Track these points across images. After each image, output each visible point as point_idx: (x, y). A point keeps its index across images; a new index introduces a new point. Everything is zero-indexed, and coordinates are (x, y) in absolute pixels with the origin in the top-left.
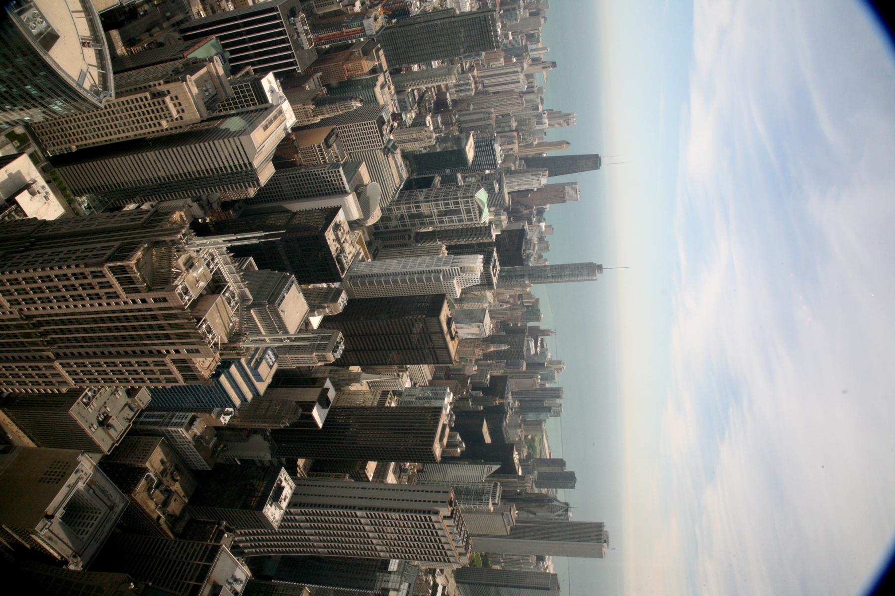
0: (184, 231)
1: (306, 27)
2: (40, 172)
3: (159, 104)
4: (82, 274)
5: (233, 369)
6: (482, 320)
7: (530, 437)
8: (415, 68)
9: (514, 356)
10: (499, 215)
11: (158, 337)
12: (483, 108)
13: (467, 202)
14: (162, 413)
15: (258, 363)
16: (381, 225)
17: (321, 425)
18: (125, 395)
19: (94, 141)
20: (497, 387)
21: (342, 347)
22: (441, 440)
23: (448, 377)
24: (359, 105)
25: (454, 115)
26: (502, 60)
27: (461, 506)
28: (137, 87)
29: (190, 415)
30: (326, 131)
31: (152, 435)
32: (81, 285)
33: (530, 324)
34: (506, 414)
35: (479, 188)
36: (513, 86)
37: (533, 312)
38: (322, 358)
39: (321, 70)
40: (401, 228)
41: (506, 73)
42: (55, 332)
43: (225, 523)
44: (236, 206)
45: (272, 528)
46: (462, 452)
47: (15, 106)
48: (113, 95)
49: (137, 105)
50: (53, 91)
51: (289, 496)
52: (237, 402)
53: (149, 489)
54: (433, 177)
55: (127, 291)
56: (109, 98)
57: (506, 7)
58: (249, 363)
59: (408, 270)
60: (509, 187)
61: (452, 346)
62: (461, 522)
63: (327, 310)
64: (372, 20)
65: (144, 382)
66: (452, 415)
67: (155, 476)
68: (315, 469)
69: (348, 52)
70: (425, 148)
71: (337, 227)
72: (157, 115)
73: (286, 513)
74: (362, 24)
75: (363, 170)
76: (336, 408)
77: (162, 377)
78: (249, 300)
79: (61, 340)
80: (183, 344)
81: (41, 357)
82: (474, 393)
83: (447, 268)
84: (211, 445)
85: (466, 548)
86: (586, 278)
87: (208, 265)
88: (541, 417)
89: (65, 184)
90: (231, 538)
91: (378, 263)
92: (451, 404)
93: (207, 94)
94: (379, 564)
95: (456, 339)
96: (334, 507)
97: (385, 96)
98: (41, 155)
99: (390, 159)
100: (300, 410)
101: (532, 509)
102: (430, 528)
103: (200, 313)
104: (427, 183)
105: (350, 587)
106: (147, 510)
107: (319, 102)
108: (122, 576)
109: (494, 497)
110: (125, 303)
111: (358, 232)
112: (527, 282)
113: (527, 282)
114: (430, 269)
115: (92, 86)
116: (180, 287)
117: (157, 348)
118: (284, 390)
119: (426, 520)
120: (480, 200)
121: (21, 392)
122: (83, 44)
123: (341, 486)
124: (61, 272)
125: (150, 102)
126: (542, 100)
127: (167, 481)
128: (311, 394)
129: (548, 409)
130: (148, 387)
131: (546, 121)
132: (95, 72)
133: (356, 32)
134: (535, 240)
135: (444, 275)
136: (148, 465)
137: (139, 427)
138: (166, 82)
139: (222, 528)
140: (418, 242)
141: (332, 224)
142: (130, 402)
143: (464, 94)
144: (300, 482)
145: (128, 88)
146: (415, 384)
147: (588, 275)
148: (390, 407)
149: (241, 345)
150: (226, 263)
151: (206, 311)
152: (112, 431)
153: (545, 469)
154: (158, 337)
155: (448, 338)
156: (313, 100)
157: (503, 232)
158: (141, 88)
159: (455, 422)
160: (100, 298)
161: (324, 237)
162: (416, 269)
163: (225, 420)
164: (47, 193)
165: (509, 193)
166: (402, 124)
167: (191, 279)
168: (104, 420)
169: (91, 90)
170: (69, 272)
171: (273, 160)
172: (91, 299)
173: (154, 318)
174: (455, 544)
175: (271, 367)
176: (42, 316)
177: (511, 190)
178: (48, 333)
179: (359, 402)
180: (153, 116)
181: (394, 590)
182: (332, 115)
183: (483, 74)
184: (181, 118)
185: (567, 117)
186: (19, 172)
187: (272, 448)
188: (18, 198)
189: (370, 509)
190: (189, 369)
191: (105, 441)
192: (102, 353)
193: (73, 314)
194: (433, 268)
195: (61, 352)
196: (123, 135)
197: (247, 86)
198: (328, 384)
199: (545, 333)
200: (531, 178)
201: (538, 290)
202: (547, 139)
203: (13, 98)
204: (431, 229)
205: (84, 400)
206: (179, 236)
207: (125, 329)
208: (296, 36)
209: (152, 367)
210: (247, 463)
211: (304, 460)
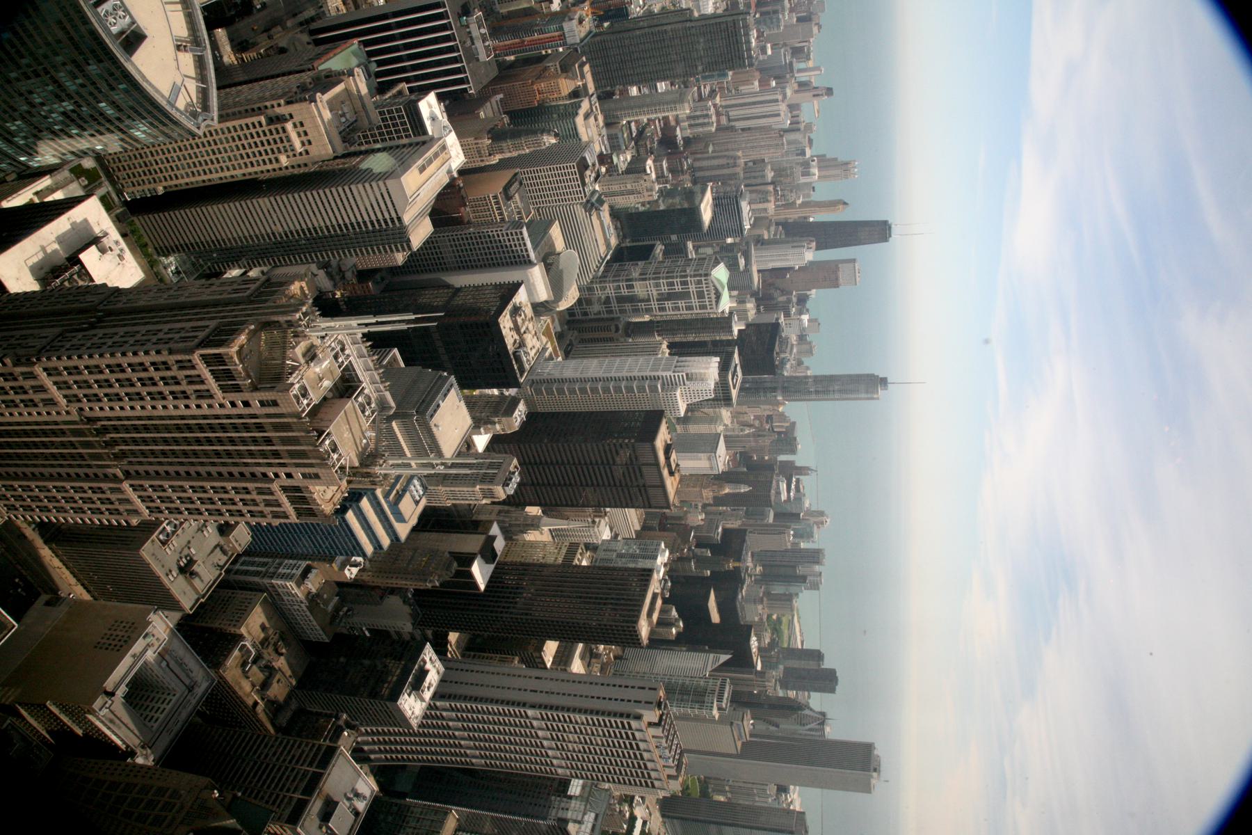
0: (304, 309)
1: (483, 31)
2: (114, 222)
3: (278, 133)
4: (164, 363)
5: (365, 503)
6: (714, 449)
7: (774, 617)
8: (634, 91)
9: (758, 500)
11: (263, 454)
12: (727, 150)
13: (699, 282)
14: (265, 560)
15: (399, 497)
17: (482, 587)
18: (216, 532)
19: (187, 180)
20: (731, 544)
21: (516, 479)
22: (650, 615)
23: (663, 528)
24: (553, 141)
25: (686, 159)
26: (756, 83)
27: (674, 710)
28: (249, 107)
29: (304, 564)
30: (507, 175)
31: (251, 590)
32: (162, 378)
33: (782, 458)
34: (743, 584)
35: (717, 263)
36: (771, 120)
37: (787, 440)
38: (489, 494)
39: (501, 90)
40: (606, 316)
42: (125, 442)
43: (345, 716)
44: (378, 276)
45: (409, 726)
46: (678, 634)
47: (85, 130)
48: (216, 118)
49: (247, 132)
50: (136, 112)
51: (435, 684)
52: (369, 549)
53: (244, 664)
54: (653, 246)
55: (224, 389)
56: (210, 123)
57: (764, 9)
58: (386, 496)
59: (613, 375)
60: (760, 262)
61: (671, 484)
63: (498, 427)
64: (575, 22)
65: (242, 515)
66: (666, 581)
67: (254, 646)
68: (472, 648)
69: (540, 66)
70: (643, 205)
72: (274, 147)
73: (430, 707)
74: (561, 28)
75: (556, 232)
76: (505, 564)
77: (268, 510)
78: (391, 408)
79: (133, 453)
80: (297, 465)
81: (106, 475)
82: (698, 551)
84: (330, 608)
85: (679, 767)
86: (863, 395)
87: (336, 357)
88: (793, 589)
89: (146, 239)
90: (352, 739)
91: (572, 363)
92: (665, 565)
93: (343, 120)
94: (556, 785)
96: (497, 702)
98: (116, 199)
99: (594, 218)
100: (455, 564)
101: (775, 719)
102: (628, 738)
103: (323, 424)
104: (644, 253)
105: (514, 814)
106: (240, 693)
107: (498, 136)
108: (203, 781)
109: (720, 699)
110: (221, 406)
111: (546, 320)
112: (780, 398)
113: (780, 398)
114: (644, 374)
115: (188, 105)
116: (297, 386)
117: (262, 469)
118: (434, 536)
120: (718, 280)
121: (76, 523)
122: (178, 48)
123: (507, 675)
124: (136, 360)
125: (265, 128)
126: (810, 141)
127: (268, 654)
128: (472, 543)
129: (803, 579)
130: (247, 523)
131: (816, 171)
132: (192, 86)
133: (552, 39)
134: (794, 339)
135: (663, 384)
136: (243, 630)
137: (232, 577)
138: (288, 103)
139: (341, 723)
141: (510, 307)
142: (222, 543)
144: (451, 665)
145: (236, 110)
146: (616, 536)
147: (867, 392)
149: (378, 470)
150: (361, 356)
151: (331, 421)
152: (196, 582)
154: (263, 454)
155: (665, 472)
156: (489, 132)
157: (748, 326)
158: (253, 110)
159: (670, 591)
160: (187, 398)
161: (498, 325)
162: (625, 374)
163: (351, 573)
164: (122, 250)
165: (759, 271)
166: (612, 169)
167: (312, 376)
168: (186, 565)
169: (186, 110)
170: (147, 360)
171: (431, 215)
172: (175, 398)
173: (260, 427)
174: (662, 762)
175: (417, 503)
176: (109, 419)
178: (114, 442)
179: (537, 557)
180: (268, 148)
181: (575, 821)
182: (515, 154)
183: (728, 103)
184: (307, 153)
185: (845, 166)
186: (86, 220)
187: (414, 616)
188: (83, 256)
189: (546, 707)
190: (304, 500)
191: (187, 595)
192: (188, 473)
193: (150, 418)
194: (648, 373)
195: (132, 469)
196: (227, 174)
197: (398, 110)
198: (495, 530)
201: (794, 410)
202: (816, 197)
203: (81, 119)
204: (647, 318)
205: (161, 537)
206: (297, 316)
207: (220, 441)
208: (469, 43)
209: (254, 496)
210: (380, 635)
211: (457, 634)
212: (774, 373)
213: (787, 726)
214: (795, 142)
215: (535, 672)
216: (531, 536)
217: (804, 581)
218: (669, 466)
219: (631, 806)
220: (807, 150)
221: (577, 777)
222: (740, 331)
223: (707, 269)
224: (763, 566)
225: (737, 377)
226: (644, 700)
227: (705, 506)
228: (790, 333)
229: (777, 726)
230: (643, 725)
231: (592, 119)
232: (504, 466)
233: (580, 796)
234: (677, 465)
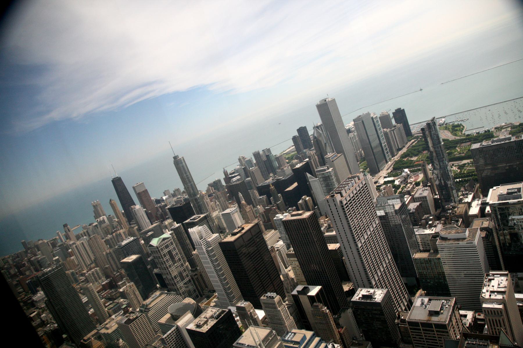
7: (287, 161)
9: (243, 187)
10: (166, 226)
12: (105, 259)
13: (162, 249)
16: (194, 295)
20: (264, 190)
21: (269, 294)
22: (300, 215)
23: (269, 220)
24: (121, 340)
25: (115, 275)
26: (72, 258)
27: (337, 186)
33: (224, 183)
35: (151, 246)
36: (86, 245)
37: (216, 185)
38: (280, 303)
40: (192, 282)
41: (79, 253)
45: (388, 291)
46: (308, 196)
54: (156, 274)
57: (39, 267)
59: (213, 270)
60: (148, 226)
61: (247, 227)
62: (341, 186)
63: (252, 311)
68: (347, 279)
71: (198, 326)
76: (307, 281)
82: (273, 202)
83: (203, 247)
86: (184, 164)
88: (273, 159)
91: (215, 288)
92: (283, 214)
97: (112, 325)
99: (151, 306)
100: (315, 304)
104: (159, 276)
109: (325, 170)
111: (202, 305)
112: (198, 196)
113: (198, 196)
114: (208, 257)
118: (308, 317)
126: (90, 225)
128: (304, 300)
129: (267, 156)
131: (101, 218)
135: (209, 247)
140: (196, 269)
141: (198, 330)
143: (100, 274)
146: (280, 238)
147: (182, 163)
148: (294, 250)
153: (301, 146)
155: (243, 231)
157: (174, 221)
161: (207, 332)
162: (211, 265)
165: (152, 224)
166: (129, 305)
174: (355, 185)
177: (150, 223)
181: (394, 207)
183: (85, 266)
185: (95, 207)
187: (344, 310)
189: (355, 240)
194: (207, 255)
200: (138, 215)
201: (202, 187)
202: (112, 214)
204: (187, 263)
210: (359, 323)
212: (189, 202)
213: (323, 140)
214: (93, 231)
216: (292, 275)
218: (240, 231)
219: (381, 186)
220: (94, 225)
223: (155, 249)
224: (269, 174)
225: (196, 217)
228: (172, 203)
229: (326, 144)
230: (343, 199)
231: (107, 326)
232: (266, 302)
233: (383, 209)
234: (239, 228)
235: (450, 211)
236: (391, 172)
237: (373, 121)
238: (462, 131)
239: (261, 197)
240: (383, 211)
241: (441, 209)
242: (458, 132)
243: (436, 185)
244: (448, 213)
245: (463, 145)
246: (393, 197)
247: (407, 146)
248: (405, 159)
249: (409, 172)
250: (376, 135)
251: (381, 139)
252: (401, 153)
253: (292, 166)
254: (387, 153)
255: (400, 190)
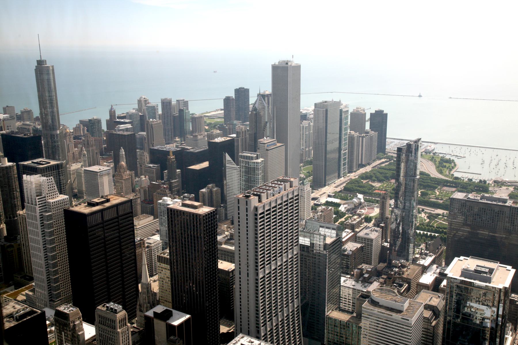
7: (207, 128)
9: (130, 143)
17: (188, 316)
20: (159, 157)
21: (111, 305)
22: (195, 207)
33: (104, 127)
37: (92, 125)
46: (216, 186)
51: (249, 339)
59: (41, 246)
61: (116, 200)
62: (264, 187)
66: (184, 197)
68: (229, 315)
82: (165, 178)
85: (285, 181)
86: (51, 76)
88: (188, 117)
92: (175, 198)
94: (305, 253)
95: (109, 197)
100: (172, 337)
101: (263, 124)
102: (269, 214)
109: (252, 158)
113: (58, 132)
114: (39, 225)
119: (263, 217)
129: (181, 111)
134: (18, 124)
140: (16, 238)
144: (239, 330)
146: (158, 231)
147: (48, 74)
148: (170, 253)
153: (233, 114)
155: (107, 205)
157: (5, 156)
162: (40, 238)
174: (283, 192)
179: (168, 281)
181: (325, 239)
194: (39, 222)
199: (112, 113)
201: (69, 121)
215: (237, 275)
216: (155, 287)
217: (183, 110)
218: (102, 203)
221: (298, 241)
222: (9, 161)
224: (175, 136)
225: (43, 162)
226: (246, 207)
227: (137, 175)
229: (267, 122)
232: (103, 314)
234: (102, 197)
235: (397, 270)
236: (340, 191)
237: (341, 115)
238: (451, 170)
239: (151, 165)
240: (309, 240)
241: (386, 264)
242: (445, 169)
243: (391, 229)
244: (392, 271)
245: (445, 188)
246: (328, 225)
247: (374, 164)
248: (364, 181)
249: (362, 200)
250: (338, 136)
251: (343, 142)
252: (362, 171)
253: (211, 136)
254: (344, 164)
255: (343, 219)
